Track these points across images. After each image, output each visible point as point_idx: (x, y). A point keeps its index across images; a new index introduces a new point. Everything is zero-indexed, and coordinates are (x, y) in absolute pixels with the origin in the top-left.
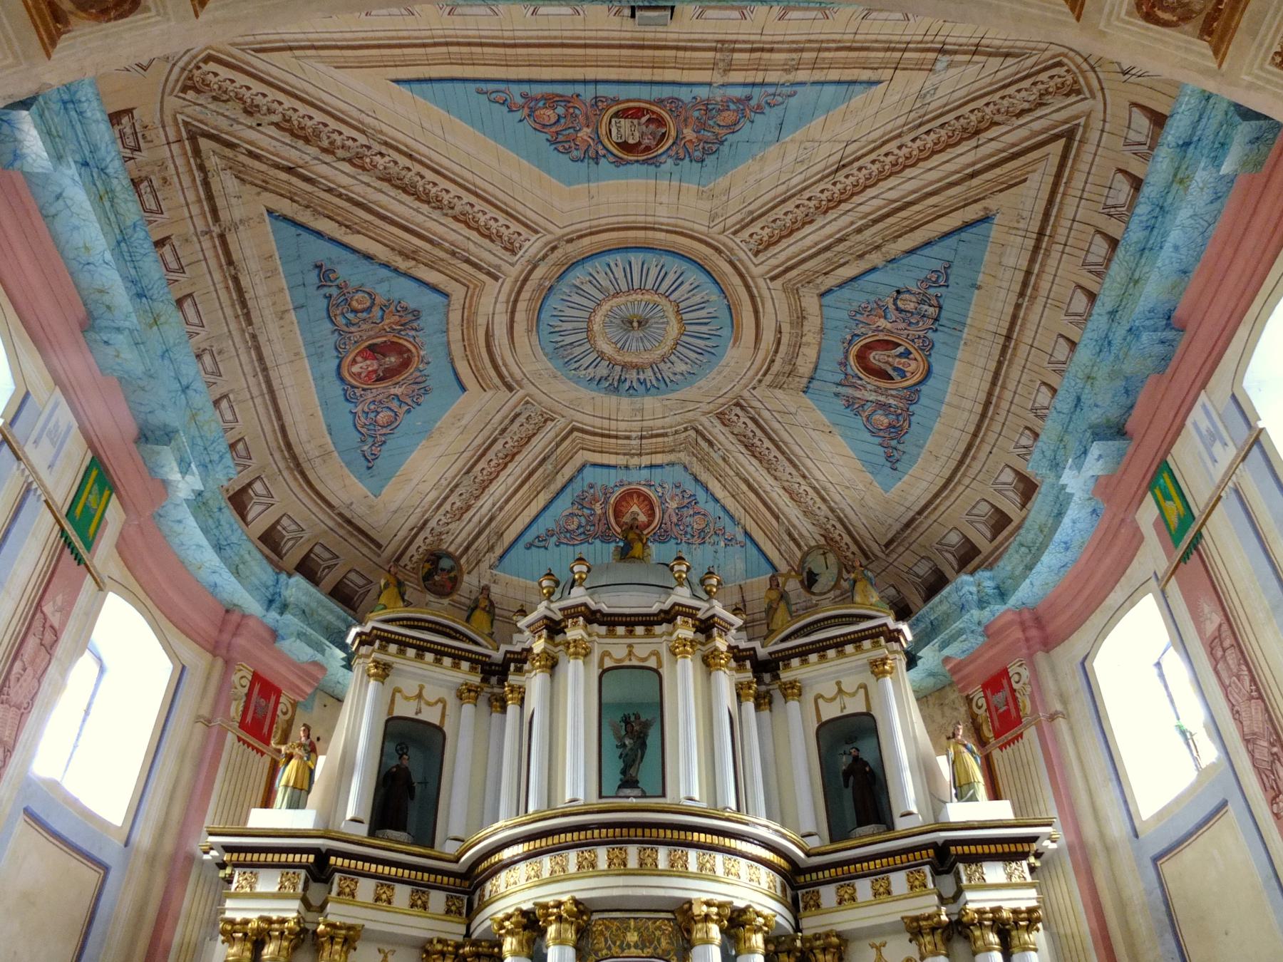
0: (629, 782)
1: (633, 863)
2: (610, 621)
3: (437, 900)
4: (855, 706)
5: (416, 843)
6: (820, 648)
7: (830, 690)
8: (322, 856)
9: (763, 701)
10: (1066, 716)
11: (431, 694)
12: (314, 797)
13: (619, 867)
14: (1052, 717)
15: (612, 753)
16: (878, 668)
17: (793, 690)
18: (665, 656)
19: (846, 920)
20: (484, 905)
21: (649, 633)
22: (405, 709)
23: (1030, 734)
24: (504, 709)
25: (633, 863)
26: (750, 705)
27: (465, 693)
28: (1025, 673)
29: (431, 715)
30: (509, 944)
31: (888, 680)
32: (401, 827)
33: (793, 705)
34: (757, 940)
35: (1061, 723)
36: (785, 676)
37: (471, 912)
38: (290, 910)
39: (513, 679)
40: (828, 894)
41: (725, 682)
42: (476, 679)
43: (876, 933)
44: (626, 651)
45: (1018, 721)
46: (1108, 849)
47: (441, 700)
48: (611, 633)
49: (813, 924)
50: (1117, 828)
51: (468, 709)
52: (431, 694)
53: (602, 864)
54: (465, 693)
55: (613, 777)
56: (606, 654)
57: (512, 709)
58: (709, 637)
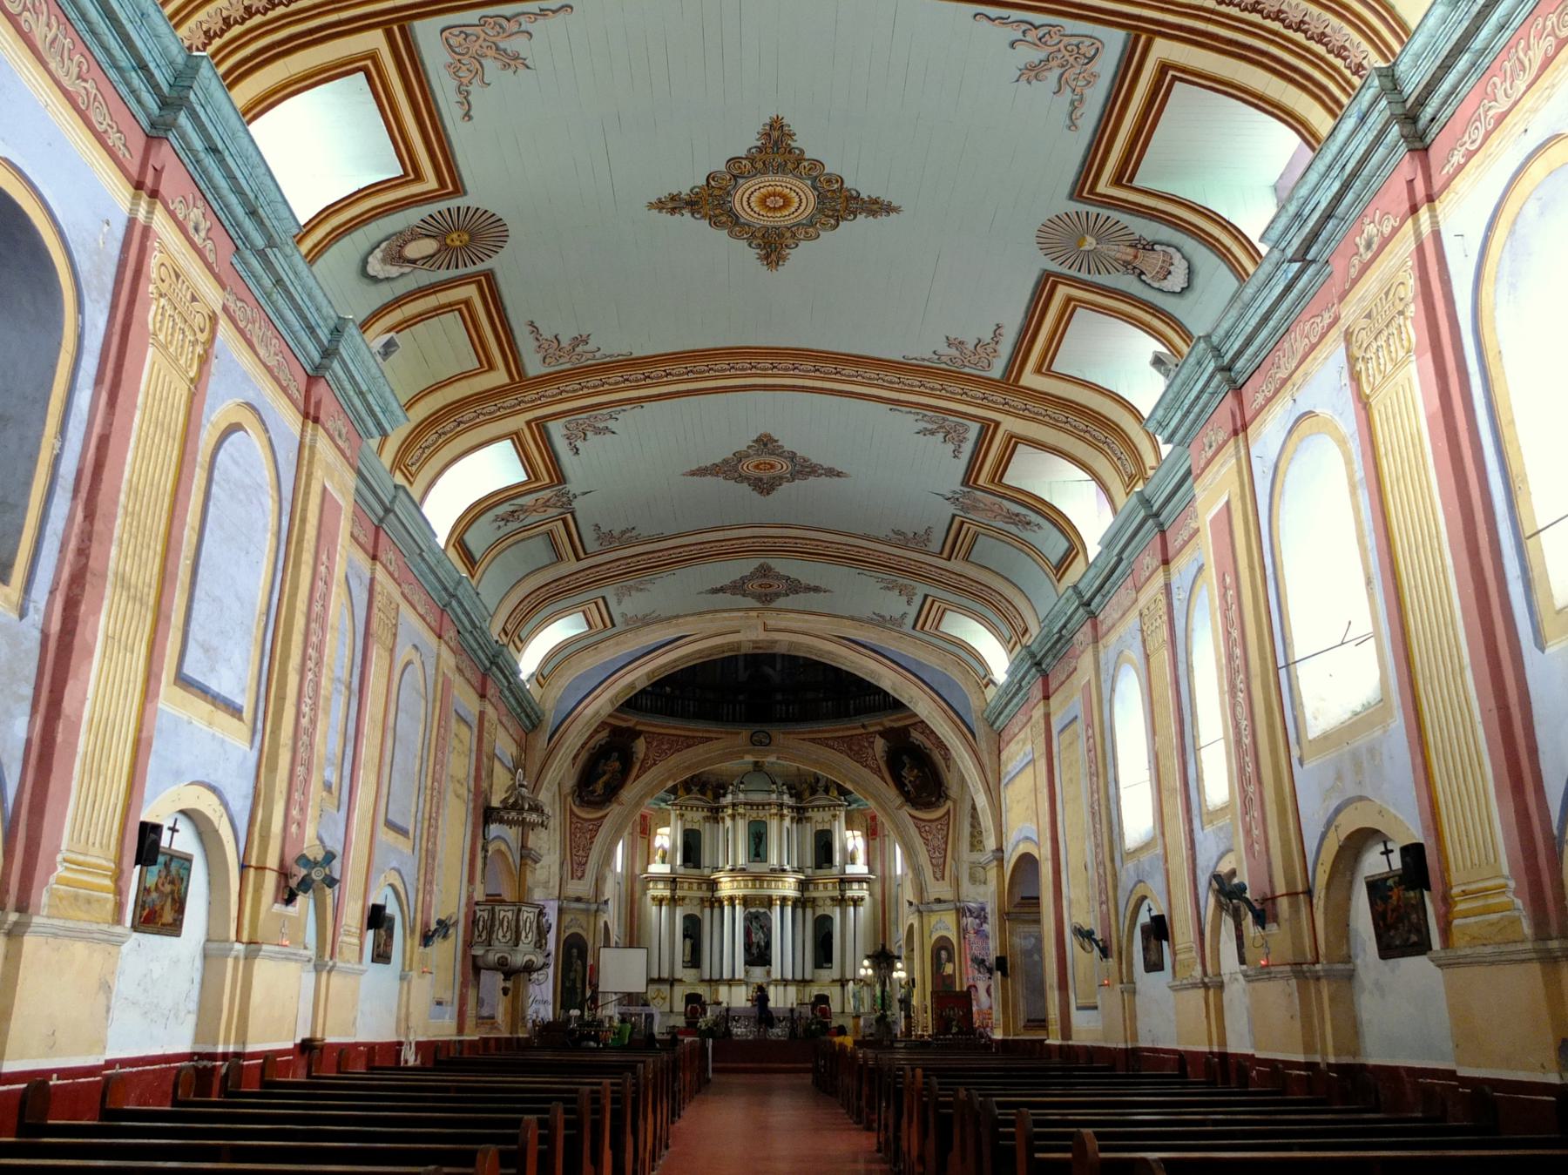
0: (757, 855)
1: (758, 886)
2: (751, 805)
3: (704, 886)
4: (827, 827)
5: (694, 867)
6: (818, 807)
8: (674, 879)
9: (799, 821)
10: (888, 836)
12: (667, 859)
13: (754, 887)
14: (884, 836)
15: (752, 843)
16: (834, 816)
17: (809, 819)
19: (815, 894)
21: (764, 809)
22: (689, 826)
24: (718, 823)
25: (758, 886)
26: (795, 825)
27: (706, 819)
29: (696, 827)
30: (726, 903)
31: (837, 823)
32: (690, 862)
33: (809, 825)
34: (790, 903)
35: (887, 839)
36: (807, 815)
37: (713, 891)
38: (667, 893)
39: (721, 815)
40: (811, 887)
41: (787, 822)
42: (709, 814)
43: (824, 899)
46: (890, 877)
48: (752, 809)
49: (807, 895)
50: (893, 874)
51: (707, 824)
53: (750, 886)
54: (706, 819)
55: (753, 852)
57: (721, 824)
58: (782, 809)
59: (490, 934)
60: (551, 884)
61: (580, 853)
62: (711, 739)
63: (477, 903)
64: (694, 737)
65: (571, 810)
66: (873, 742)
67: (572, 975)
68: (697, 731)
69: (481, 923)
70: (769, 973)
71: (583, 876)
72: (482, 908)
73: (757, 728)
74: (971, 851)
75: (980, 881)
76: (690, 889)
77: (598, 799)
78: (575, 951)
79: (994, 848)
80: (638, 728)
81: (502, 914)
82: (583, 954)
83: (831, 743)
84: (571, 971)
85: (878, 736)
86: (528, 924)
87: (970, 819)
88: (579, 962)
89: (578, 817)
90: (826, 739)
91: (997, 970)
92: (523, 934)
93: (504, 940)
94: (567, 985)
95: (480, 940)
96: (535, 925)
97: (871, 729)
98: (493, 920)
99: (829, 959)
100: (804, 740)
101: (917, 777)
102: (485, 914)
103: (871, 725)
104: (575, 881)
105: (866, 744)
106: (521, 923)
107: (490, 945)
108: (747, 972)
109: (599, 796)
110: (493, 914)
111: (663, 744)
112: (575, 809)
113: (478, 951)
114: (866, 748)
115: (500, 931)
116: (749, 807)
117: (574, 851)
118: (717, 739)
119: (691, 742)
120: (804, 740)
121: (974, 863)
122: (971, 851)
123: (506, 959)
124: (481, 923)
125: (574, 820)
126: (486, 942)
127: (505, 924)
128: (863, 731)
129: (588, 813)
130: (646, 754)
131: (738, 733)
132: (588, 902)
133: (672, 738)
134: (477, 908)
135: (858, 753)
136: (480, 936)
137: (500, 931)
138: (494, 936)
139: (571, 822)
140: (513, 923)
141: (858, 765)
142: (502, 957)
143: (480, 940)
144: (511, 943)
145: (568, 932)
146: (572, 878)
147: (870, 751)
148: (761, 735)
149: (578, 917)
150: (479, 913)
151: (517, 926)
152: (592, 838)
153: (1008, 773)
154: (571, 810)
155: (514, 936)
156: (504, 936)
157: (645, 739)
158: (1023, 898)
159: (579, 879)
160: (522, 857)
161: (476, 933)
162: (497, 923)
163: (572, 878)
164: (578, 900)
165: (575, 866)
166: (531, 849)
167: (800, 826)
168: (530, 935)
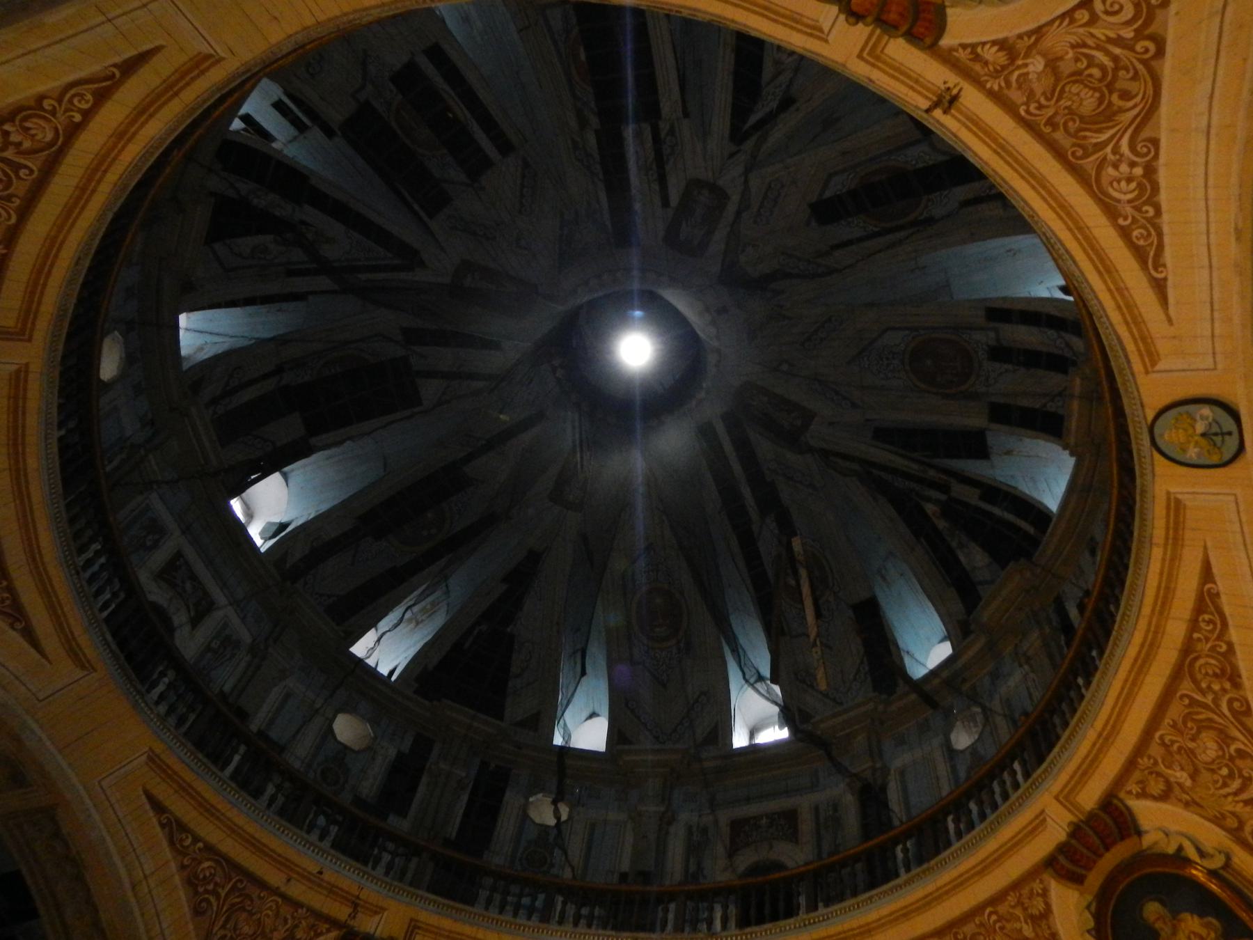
62: (1207, 602)
64: (1187, 649)
66: (1002, 44)
80: (1090, 797)
83: (1123, 193)
85: (946, 41)
90: (1111, 211)
97: (937, 74)
100: (1160, 287)
103: (915, 82)
105: (1036, 65)
111: (1191, 753)
114: (1052, 64)
118: (1207, 573)
119: (1206, 663)
120: (1160, 287)
128: (972, 99)
130: (1218, 820)
131: (1176, 507)
133: (1176, 711)
135: (1108, 84)
141: (1167, 68)
147: (1060, 40)
157: (1143, 795)
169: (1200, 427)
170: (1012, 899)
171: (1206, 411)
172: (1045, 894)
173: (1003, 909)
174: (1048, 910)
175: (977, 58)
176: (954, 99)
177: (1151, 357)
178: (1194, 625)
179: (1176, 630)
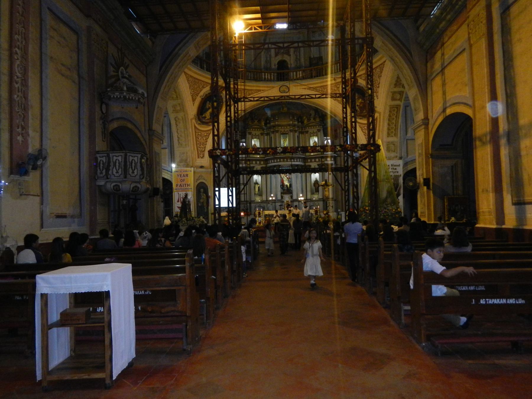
7: (312, 132)
11: (257, 134)
17: (307, 132)
18: (289, 131)
20: (268, 164)
23: (338, 139)
28: (339, 131)
33: (307, 134)
37: (266, 164)
42: (263, 132)
44: (283, 131)
45: (337, 137)
47: (258, 135)
48: (282, 128)
52: (257, 134)
56: (281, 131)
59: (107, 170)
60: (188, 160)
61: (202, 146)
63: (98, 152)
64: (251, 90)
65: (195, 127)
67: (202, 201)
68: (254, 86)
69: (101, 165)
70: (292, 197)
71: (203, 156)
72: (101, 155)
73: (282, 83)
74: (388, 137)
75: (392, 151)
76: (256, 163)
77: (207, 121)
78: (202, 190)
79: (423, 118)
81: (115, 158)
82: (206, 191)
84: (201, 199)
86: (133, 164)
87: (387, 121)
88: (204, 195)
89: (199, 130)
90: (316, 87)
91: (425, 185)
92: (131, 171)
93: (117, 175)
94: (200, 205)
95: (101, 175)
96: (139, 164)
98: (109, 162)
99: (317, 191)
101: (361, 103)
102: (104, 159)
104: (200, 159)
106: (128, 163)
107: (108, 178)
108: (282, 197)
109: (208, 119)
110: (109, 158)
112: (197, 126)
113: (101, 183)
115: (114, 170)
116: (280, 128)
117: (198, 145)
120: (305, 89)
121: (389, 142)
122: (388, 137)
123: (119, 186)
124: (101, 165)
125: (197, 131)
126: (105, 177)
127: (117, 164)
129: (204, 127)
131: (273, 87)
132: (207, 168)
134: (98, 155)
136: (101, 173)
137: (114, 170)
138: (110, 172)
139: (195, 132)
140: (123, 164)
142: (116, 185)
143: (101, 175)
144: (122, 176)
145: (199, 182)
146: (198, 158)
148: (284, 87)
149: (202, 175)
150: (99, 159)
151: (125, 165)
152: (207, 139)
153: (432, 74)
154: (195, 127)
155: (123, 173)
156: (117, 172)
158: (441, 145)
159: (202, 158)
160: (149, 135)
161: (99, 171)
162: (112, 164)
163: (198, 158)
164: (202, 167)
165: (199, 152)
166: (154, 131)
167: (303, 135)
168: (136, 171)
169: (285, 90)
170: (204, 83)
171: (288, 91)
172: (207, 86)
173: (202, 83)
174: (205, 87)
175: (338, 85)
176: (334, 80)
177: (295, 86)
178: (256, 90)
179: (255, 88)
